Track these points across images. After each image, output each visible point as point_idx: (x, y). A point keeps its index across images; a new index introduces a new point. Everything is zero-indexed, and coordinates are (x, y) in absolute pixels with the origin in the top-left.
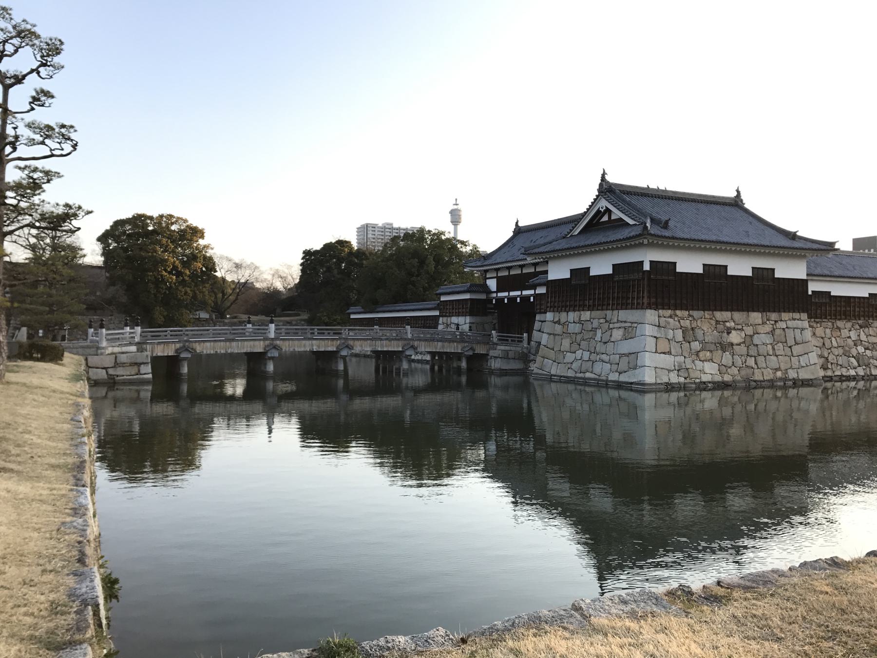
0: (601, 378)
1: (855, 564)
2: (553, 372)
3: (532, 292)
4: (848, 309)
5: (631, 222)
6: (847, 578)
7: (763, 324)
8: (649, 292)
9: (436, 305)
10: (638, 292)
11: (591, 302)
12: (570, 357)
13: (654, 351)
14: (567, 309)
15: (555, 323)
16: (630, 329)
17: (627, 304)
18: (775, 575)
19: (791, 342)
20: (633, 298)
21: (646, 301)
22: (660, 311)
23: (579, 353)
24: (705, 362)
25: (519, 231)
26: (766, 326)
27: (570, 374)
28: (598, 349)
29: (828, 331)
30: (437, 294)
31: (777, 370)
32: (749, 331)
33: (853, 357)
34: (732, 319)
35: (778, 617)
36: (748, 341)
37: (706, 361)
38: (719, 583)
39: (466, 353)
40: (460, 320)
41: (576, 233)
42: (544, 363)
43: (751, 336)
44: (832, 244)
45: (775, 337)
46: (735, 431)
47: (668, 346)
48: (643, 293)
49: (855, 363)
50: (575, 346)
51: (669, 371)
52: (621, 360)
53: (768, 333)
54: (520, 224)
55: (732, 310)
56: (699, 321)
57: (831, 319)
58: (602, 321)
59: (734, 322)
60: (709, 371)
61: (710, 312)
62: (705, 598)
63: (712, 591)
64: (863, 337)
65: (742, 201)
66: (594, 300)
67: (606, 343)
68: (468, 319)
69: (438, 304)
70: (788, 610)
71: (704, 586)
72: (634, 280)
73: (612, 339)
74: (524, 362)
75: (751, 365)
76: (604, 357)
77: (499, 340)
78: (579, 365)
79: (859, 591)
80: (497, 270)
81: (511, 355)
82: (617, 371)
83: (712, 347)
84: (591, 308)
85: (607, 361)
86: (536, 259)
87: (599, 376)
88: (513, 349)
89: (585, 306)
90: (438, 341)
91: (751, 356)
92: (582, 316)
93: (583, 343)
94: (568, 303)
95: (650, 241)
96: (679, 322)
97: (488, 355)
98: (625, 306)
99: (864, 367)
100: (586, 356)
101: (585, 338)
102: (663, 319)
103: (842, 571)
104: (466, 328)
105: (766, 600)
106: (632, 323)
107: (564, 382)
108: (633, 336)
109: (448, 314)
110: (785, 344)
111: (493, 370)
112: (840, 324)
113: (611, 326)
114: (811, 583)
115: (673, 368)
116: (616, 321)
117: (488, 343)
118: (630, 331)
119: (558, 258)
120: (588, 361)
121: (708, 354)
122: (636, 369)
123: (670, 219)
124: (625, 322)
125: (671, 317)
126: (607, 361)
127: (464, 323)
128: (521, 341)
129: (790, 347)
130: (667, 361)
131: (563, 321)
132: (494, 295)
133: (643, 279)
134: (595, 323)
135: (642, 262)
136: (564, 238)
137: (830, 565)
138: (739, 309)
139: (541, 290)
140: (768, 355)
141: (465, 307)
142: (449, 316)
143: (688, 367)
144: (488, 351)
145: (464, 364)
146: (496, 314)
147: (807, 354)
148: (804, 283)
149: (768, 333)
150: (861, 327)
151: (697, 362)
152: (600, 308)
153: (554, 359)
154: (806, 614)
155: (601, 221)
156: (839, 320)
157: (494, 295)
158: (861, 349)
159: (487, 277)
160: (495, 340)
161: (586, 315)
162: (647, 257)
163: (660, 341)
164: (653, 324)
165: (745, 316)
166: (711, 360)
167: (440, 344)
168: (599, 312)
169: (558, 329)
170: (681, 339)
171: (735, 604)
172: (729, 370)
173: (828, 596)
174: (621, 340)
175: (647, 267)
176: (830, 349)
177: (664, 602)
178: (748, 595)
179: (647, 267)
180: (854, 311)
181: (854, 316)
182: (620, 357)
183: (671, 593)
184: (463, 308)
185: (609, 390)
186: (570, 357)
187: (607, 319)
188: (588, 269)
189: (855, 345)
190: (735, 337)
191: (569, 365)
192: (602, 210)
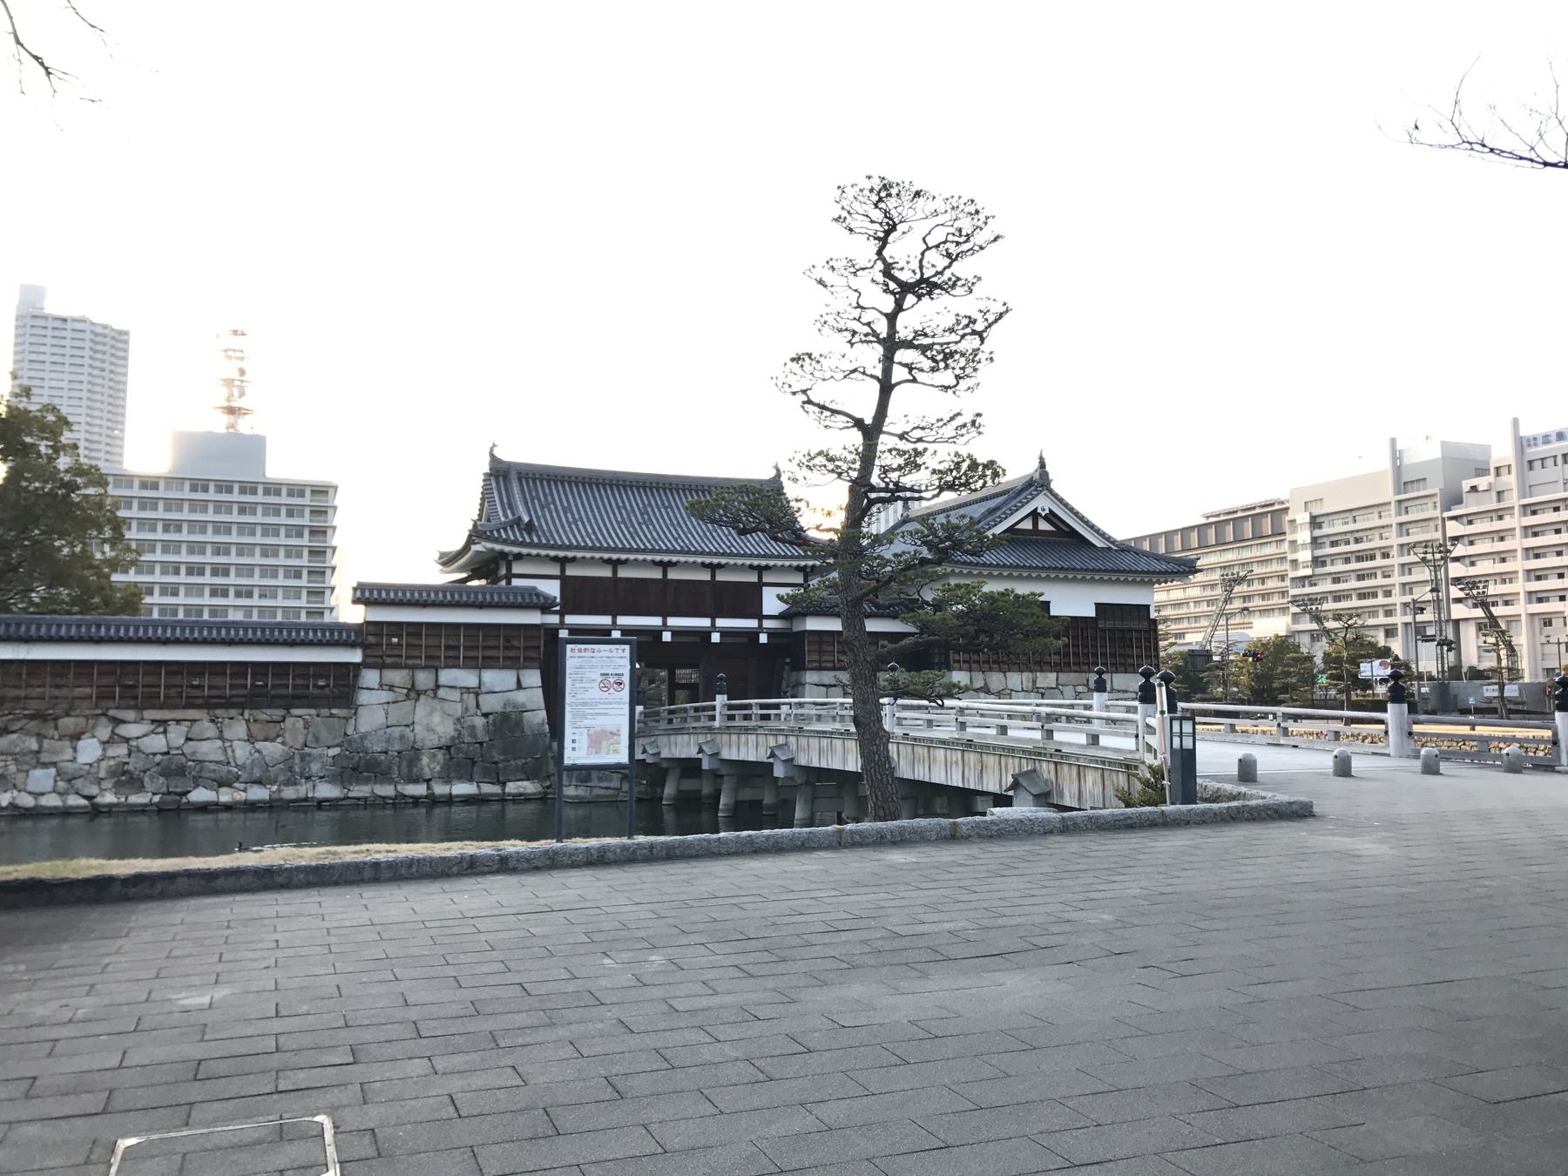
5: (1098, 543)
10: (1148, 649)
80: (563, 562)
142: (426, 667)
168: (1073, 675)
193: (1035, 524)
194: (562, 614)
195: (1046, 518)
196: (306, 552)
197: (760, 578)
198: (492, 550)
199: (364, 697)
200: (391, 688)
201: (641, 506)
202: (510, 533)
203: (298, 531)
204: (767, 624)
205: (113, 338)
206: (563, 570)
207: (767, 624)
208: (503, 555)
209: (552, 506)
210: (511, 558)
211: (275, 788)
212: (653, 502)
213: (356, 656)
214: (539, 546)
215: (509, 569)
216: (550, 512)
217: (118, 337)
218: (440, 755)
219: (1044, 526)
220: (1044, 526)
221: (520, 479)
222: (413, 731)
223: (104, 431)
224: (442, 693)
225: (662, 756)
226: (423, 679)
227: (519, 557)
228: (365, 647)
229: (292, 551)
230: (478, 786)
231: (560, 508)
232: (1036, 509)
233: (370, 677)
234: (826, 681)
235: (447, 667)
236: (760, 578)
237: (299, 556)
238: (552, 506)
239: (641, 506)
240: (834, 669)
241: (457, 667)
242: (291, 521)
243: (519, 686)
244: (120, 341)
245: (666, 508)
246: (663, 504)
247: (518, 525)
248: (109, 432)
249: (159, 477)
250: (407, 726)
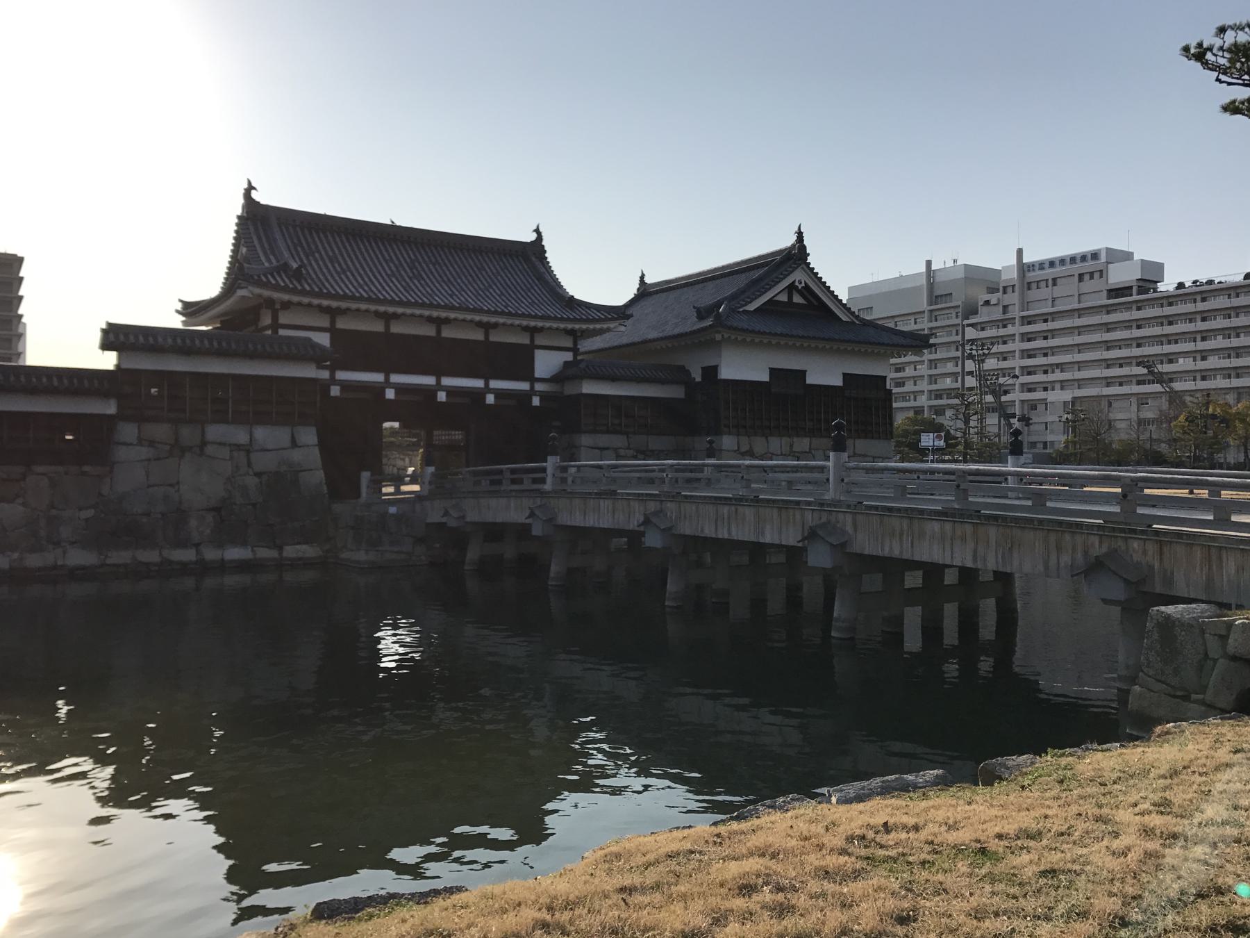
80: (333, 313)
95: (726, 336)
188: (803, 373)
193: (790, 297)
194: (333, 371)
195: (800, 292)
197: (532, 340)
198: (260, 296)
199: (121, 453)
200: (152, 443)
201: (408, 260)
202: (278, 279)
204: (539, 387)
206: (333, 322)
207: (539, 387)
208: (270, 303)
209: (317, 255)
210: (278, 306)
211: (16, 555)
212: (419, 257)
213: (110, 408)
214: (311, 294)
215: (275, 318)
216: (316, 261)
218: (210, 518)
219: (797, 299)
220: (797, 299)
221: (280, 227)
222: (178, 490)
224: (210, 450)
225: (468, 519)
226: (188, 434)
227: (286, 305)
230: (253, 551)
231: (325, 257)
232: (794, 282)
234: (601, 445)
235: (214, 422)
236: (532, 340)
238: (317, 255)
239: (408, 260)
240: (608, 432)
241: (226, 422)
243: (294, 444)
245: (434, 265)
246: (431, 261)
247: (285, 272)
250: (171, 485)
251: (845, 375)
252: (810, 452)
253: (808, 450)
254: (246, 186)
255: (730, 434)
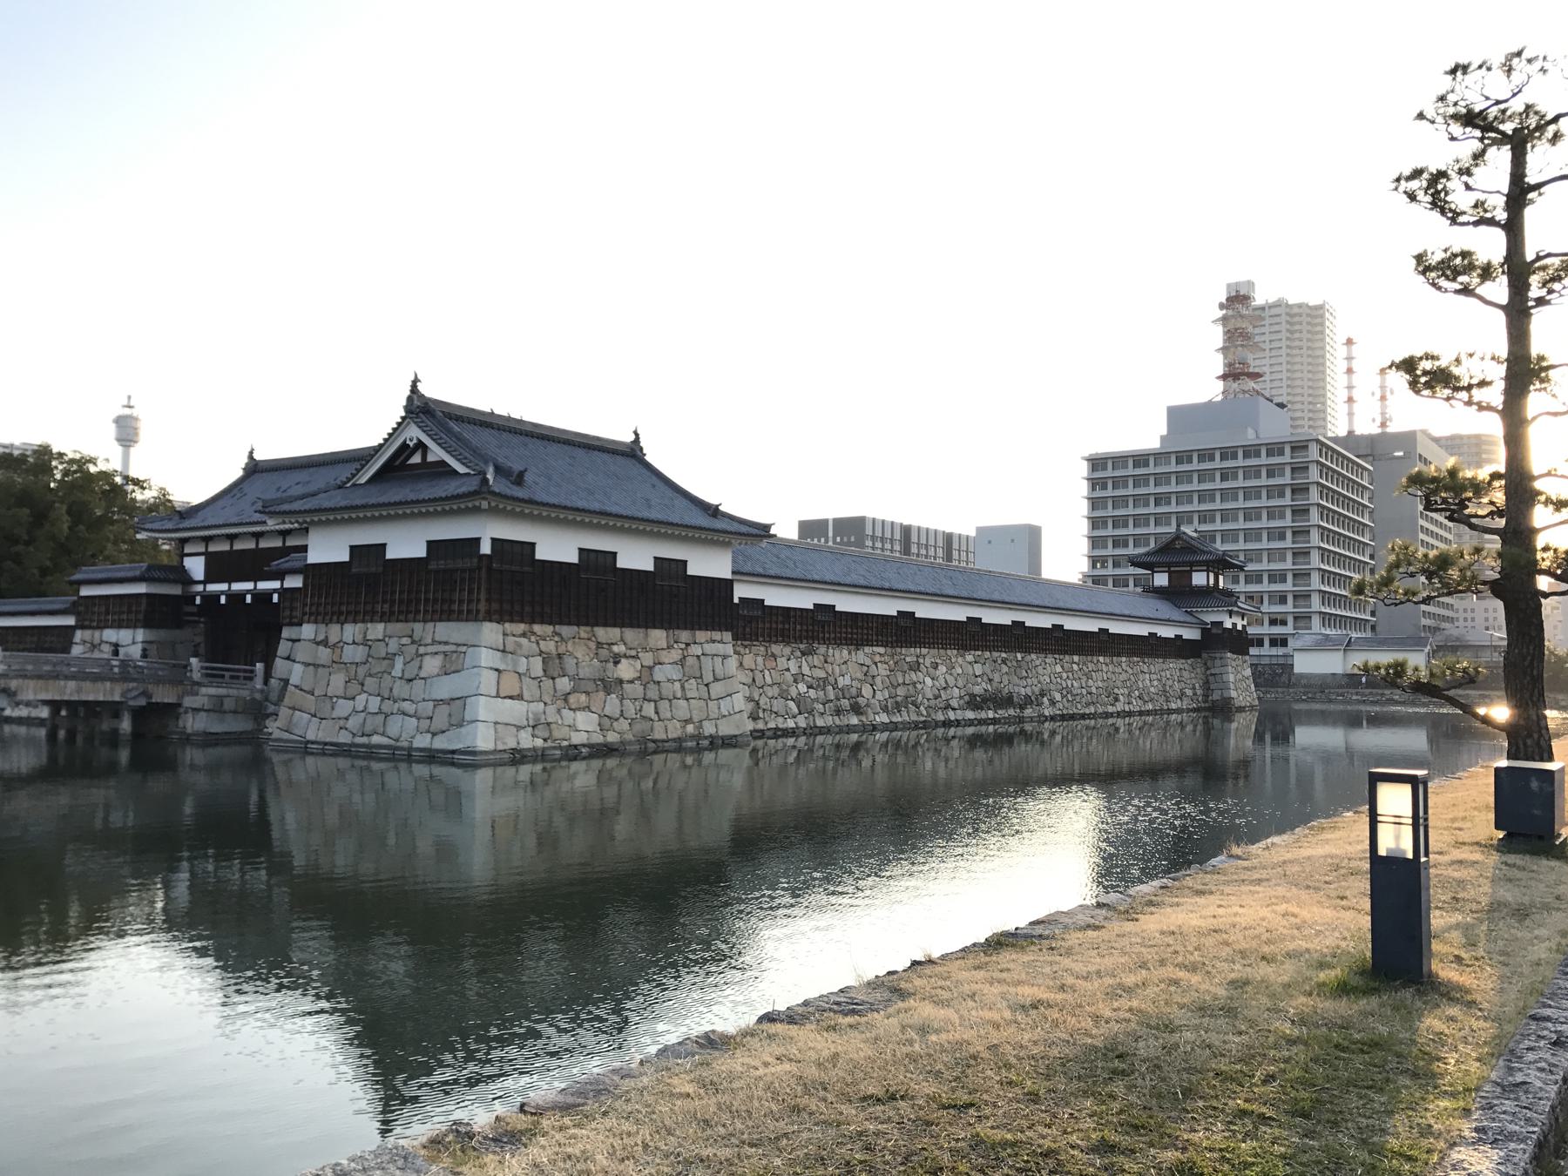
0: (399, 744)
1: (738, 1040)
2: (311, 736)
3: (276, 585)
4: (787, 626)
5: (461, 469)
6: (724, 1064)
7: (668, 648)
8: (489, 591)
9: (68, 605)
10: (471, 592)
11: (386, 606)
12: (343, 707)
13: (494, 694)
14: (343, 618)
15: (318, 643)
16: (455, 655)
17: (451, 611)
18: (615, 1078)
19: (708, 677)
20: (461, 602)
21: (483, 606)
22: (507, 625)
23: (361, 699)
24: (578, 713)
25: (255, 469)
26: (672, 651)
27: (344, 738)
28: (396, 692)
29: (760, 659)
30: (72, 583)
31: (687, 722)
32: (648, 659)
33: (792, 699)
34: (622, 640)
35: (605, 1152)
36: (646, 676)
37: (579, 709)
38: (522, 1108)
39: (131, 703)
40: (123, 636)
41: (363, 480)
42: (295, 719)
43: (651, 668)
44: (767, 528)
45: (686, 669)
46: (623, 827)
47: (518, 685)
48: (478, 593)
49: (796, 710)
50: (354, 688)
51: (519, 728)
52: (437, 710)
53: (676, 663)
54: (258, 456)
55: (622, 626)
56: (570, 643)
57: (764, 641)
58: (405, 641)
59: (625, 644)
60: (583, 727)
61: (588, 629)
62: (494, 1140)
63: (508, 1124)
64: (805, 670)
65: (641, 449)
66: (393, 602)
67: (411, 680)
68: (140, 634)
69: (74, 603)
70: (624, 1136)
71: (497, 1117)
72: (463, 571)
73: (422, 675)
74: (255, 719)
75: (648, 715)
76: (406, 706)
77: (203, 675)
78: (361, 721)
79: (736, 1085)
81: (229, 704)
82: (428, 732)
83: (590, 686)
84: (386, 618)
85: (412, 712)
86: (284, 523)
87: (397, 740)
88: (233, 693)
89: (374, 613)
90: (67, 678)
91: (650, 701)
92: (369, 632)
93: (369, 681)
94: (344, 608)
95: (493, 504)
96: (538, 643)
97: (179, 705)
98: (448, 615)
99: (806, 715)
100: (374, 704)
101: (374, 671)
102: (511, 639)
103: (717, 1053)
104: (136, 652)
105: (594, 1125)
106: (458, 645)
107: (331, 755)
108: (460, 667)
109: (95, 624)
110: (699, 681)
111: (189, 735)
112: (776, 649)
113: (422, 650)
114: (668, 1081)
115: (525, 723)
116: (430, 641)
117: (181, 683)
118: (453, 658)
119: (328, 523)
120: (377, 713)
121: (583, 697)
122: (461, 726)
123: (526, 470)
124: (446, 643)
125: (524, 635)
126: (412, 712)
127: (130, 642)
128: (251, 679)
129: (707, 685)
130: (515, 711)
131: (333, 639)
132: (200, 588)
133: (480, 568)
134: (393, 646)
135: (478, 540)
136: (340, 487)
137: (701, 1046)
138: (633, 624)
139: (294, 582)
140: (675, 698)
141: (134, 609)
143: (550, 720)
144: (181, 697)
145: (126, 725)
146: (202, 625)
147: (730, 695)
148: (727, 585)
149: (676, 663)
150: (803, 654)
151: (565, 712)
152: (400, 617)
153: (313, 711)
154: (649, 1138)
155: (409, 462)
156: (775, 642)
157: (200, 588)
158: (802, 688)
159: (186, 551)
160: (196, 676)
161: (377, 630)
162: (488, 531)
163: (504, 676)
164: (494, 647)
165: (642, 635)
166: (587, 708)
167: (72, 684)
168: (399, 625)
169: (324, 654)
170: (540, 673)
171: (542, 1141)
172: (615, 724)
173: (690, 1099)
174: (438, 675)
175: (486, 548)
176: (762, 687)
177: (419, 1162)
178: (567, 1121)
179: (486, 548)
180: (795, 630)
181: (795, 638)
182: (435, 706)
183: (435, 1143)
184: (129, 612)
185: (414, 765)
186: (343, 707)
187: (416, 638)
188: (382, 547)
189: (796, 681)
190: (626, 670)
191: (342, 723)
192: (411, 444)
193: (424, 456)
196: (1288, 513)
203: (1279, 491)
205: (1308, 315)
217: (1315, 313)
223: (1306, 407)
228: (78, 614)
229: (1273, 513)
232: (405, 441)
233: (79, 635)
237: (1282, 517)
242: (1272, 482)
244: (1316, 317)
248: (1311, 407)
249: (1148, 455)
251: (429, 543)
252: (383, 640)
253: (381, 638)
254: (249, 450)
255: (309, 622)
